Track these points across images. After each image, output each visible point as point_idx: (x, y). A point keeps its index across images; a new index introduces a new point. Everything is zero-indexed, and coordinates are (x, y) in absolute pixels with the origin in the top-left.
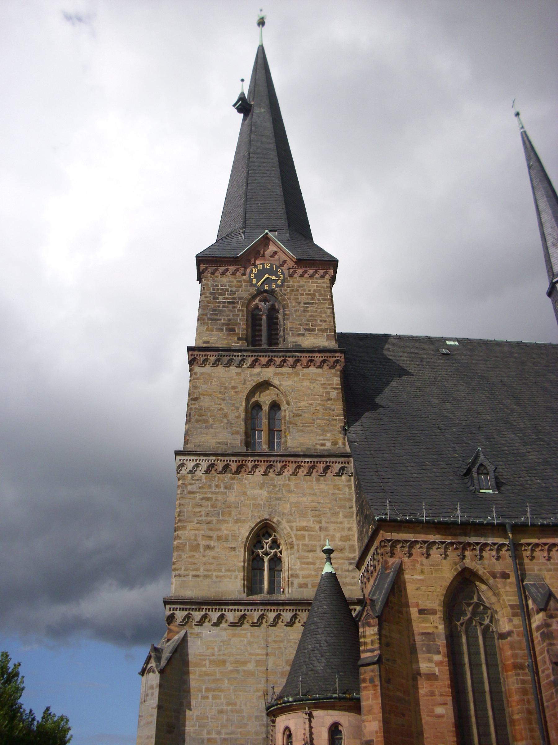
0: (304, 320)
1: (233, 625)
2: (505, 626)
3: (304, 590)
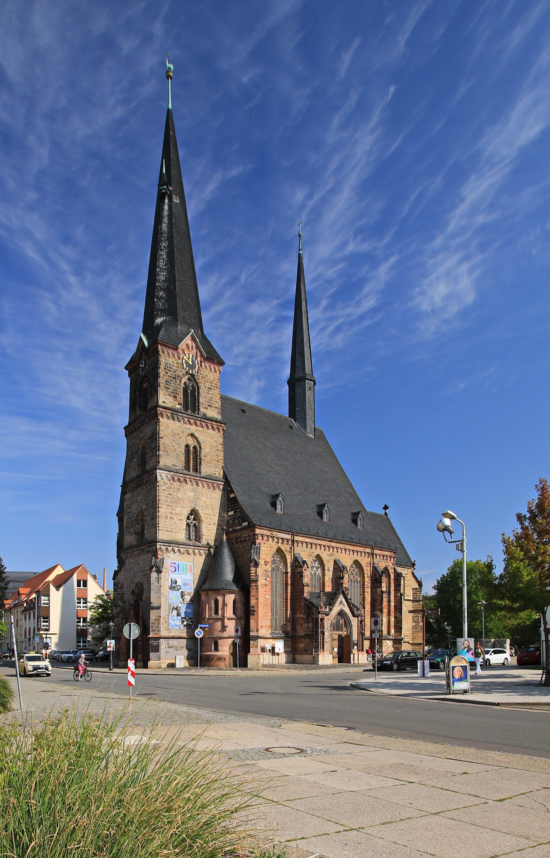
0: (208, 400)
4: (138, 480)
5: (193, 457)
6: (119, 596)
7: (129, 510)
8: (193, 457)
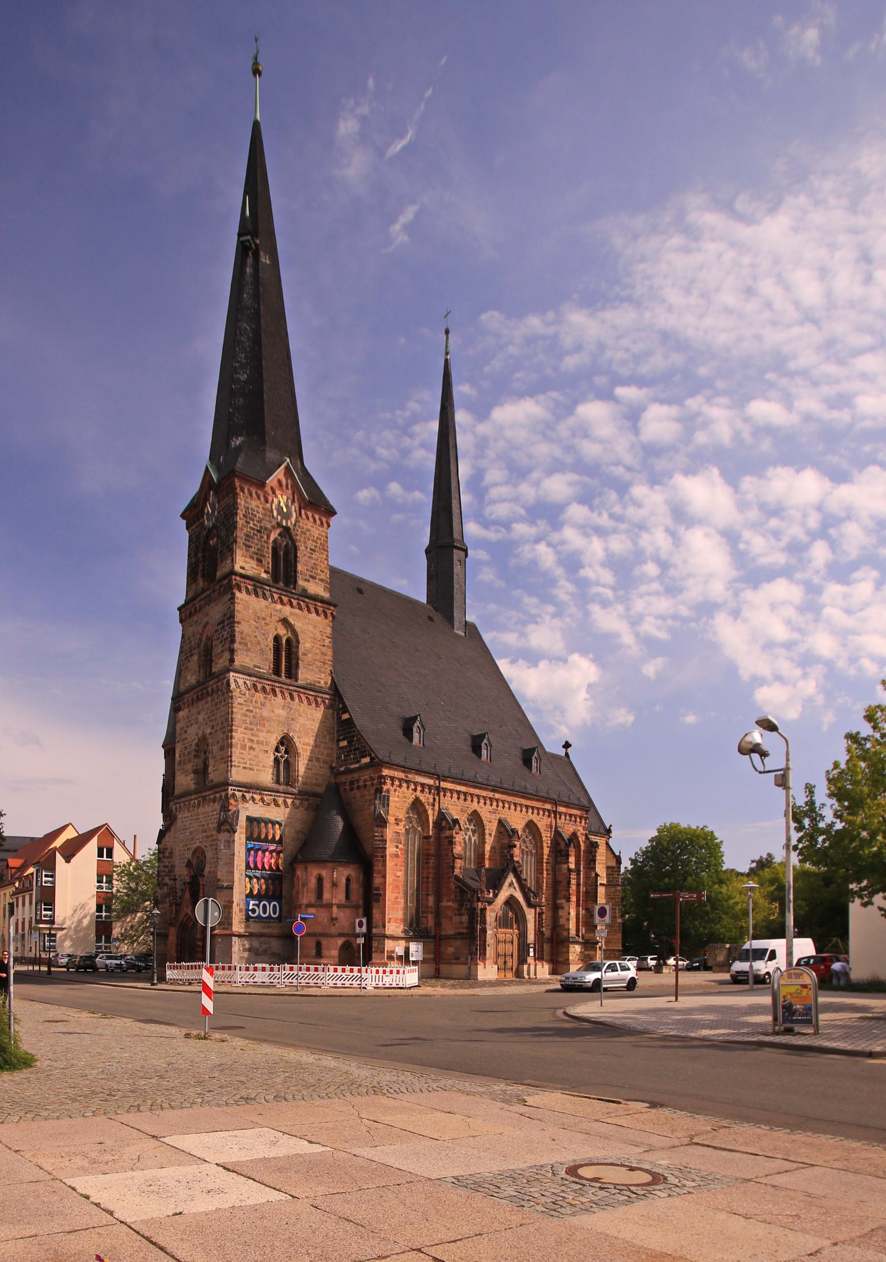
0: (309, 568)
4: (199, 688)
5: (286, 655)
6: (167, 870)
7: (184, 736)
8: (286, 655)
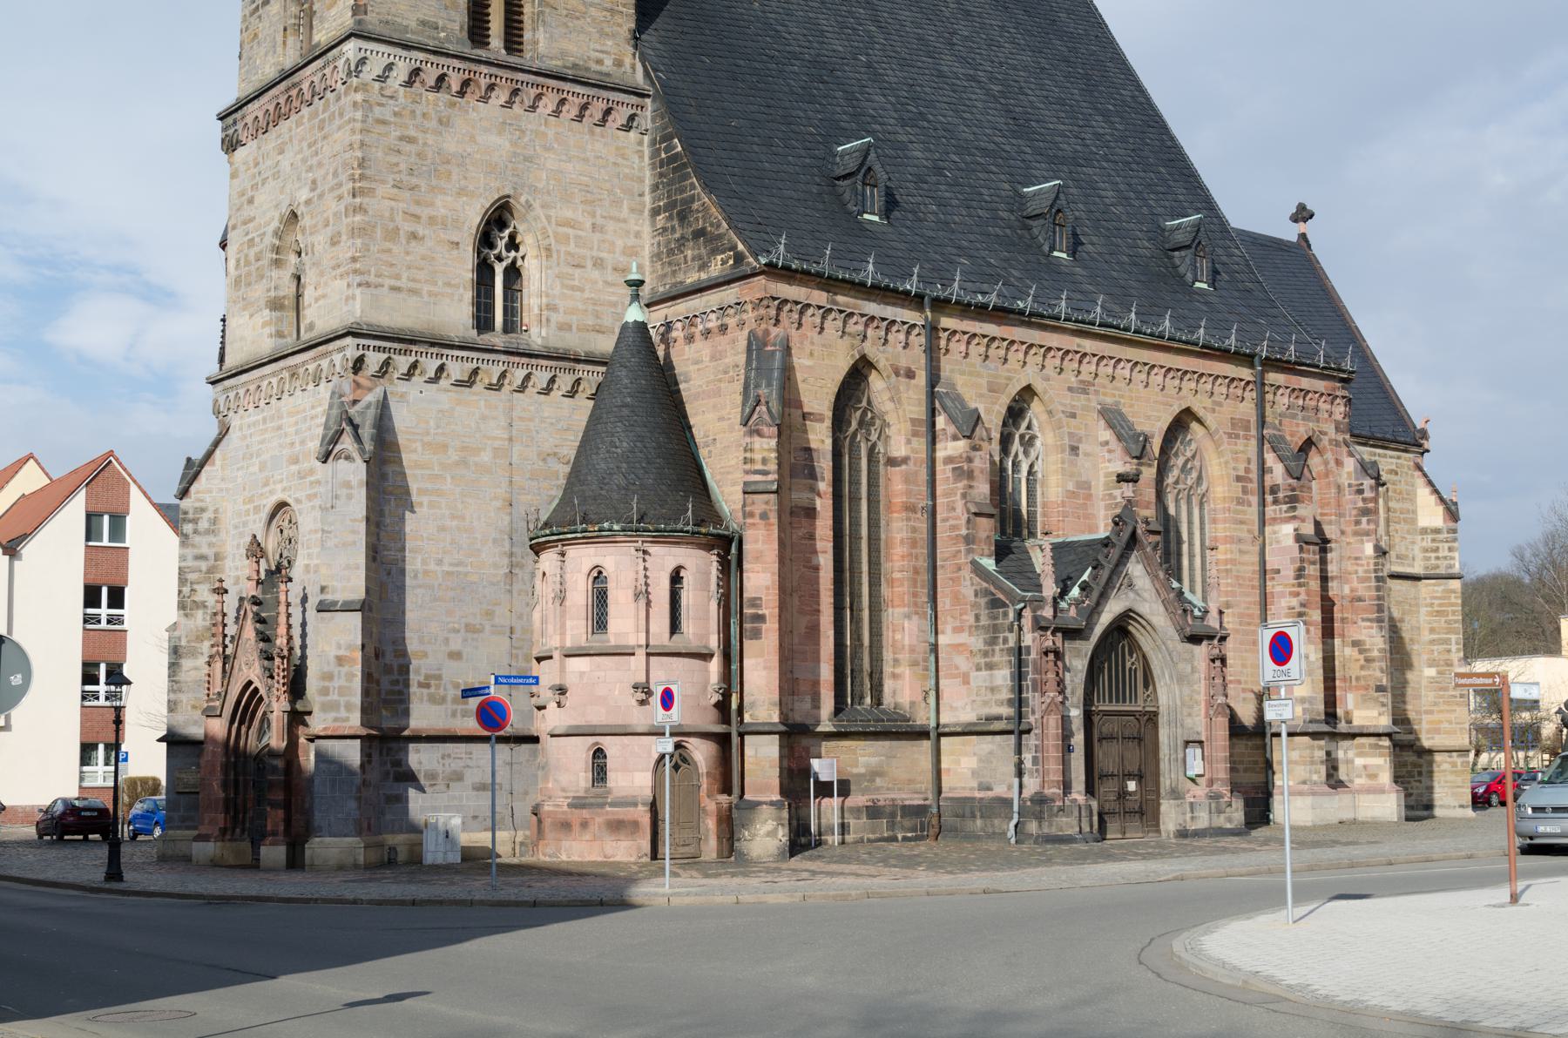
1: (459, 384)
2: (898, 448)
3: (567, 335)
